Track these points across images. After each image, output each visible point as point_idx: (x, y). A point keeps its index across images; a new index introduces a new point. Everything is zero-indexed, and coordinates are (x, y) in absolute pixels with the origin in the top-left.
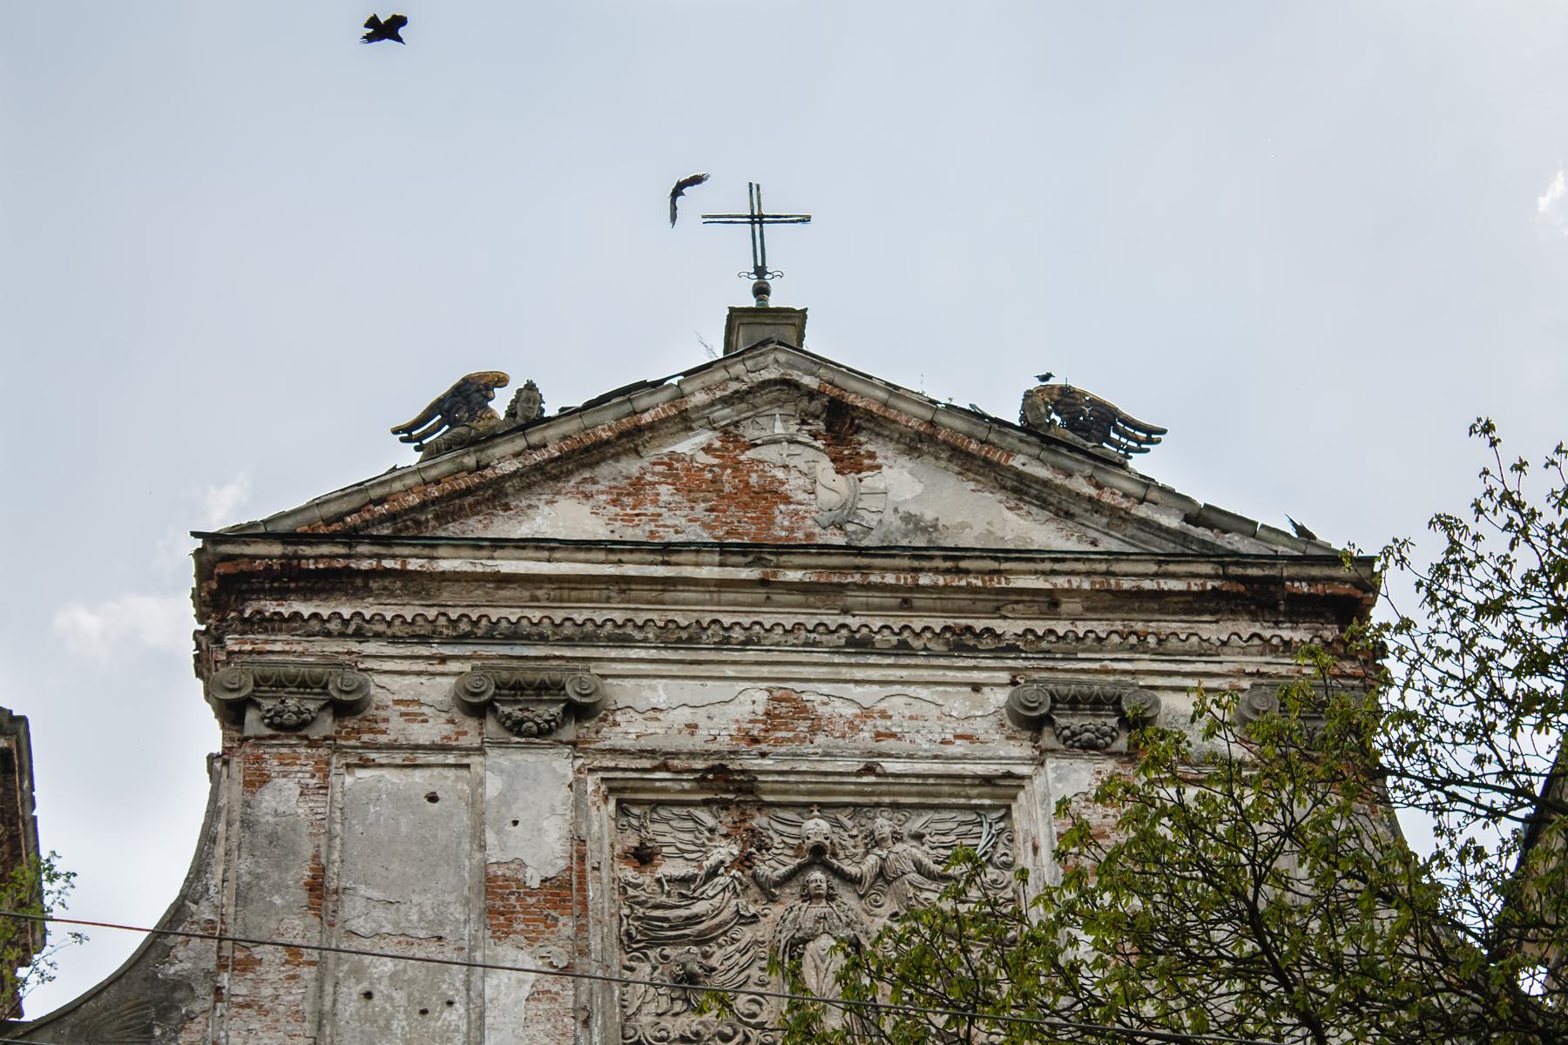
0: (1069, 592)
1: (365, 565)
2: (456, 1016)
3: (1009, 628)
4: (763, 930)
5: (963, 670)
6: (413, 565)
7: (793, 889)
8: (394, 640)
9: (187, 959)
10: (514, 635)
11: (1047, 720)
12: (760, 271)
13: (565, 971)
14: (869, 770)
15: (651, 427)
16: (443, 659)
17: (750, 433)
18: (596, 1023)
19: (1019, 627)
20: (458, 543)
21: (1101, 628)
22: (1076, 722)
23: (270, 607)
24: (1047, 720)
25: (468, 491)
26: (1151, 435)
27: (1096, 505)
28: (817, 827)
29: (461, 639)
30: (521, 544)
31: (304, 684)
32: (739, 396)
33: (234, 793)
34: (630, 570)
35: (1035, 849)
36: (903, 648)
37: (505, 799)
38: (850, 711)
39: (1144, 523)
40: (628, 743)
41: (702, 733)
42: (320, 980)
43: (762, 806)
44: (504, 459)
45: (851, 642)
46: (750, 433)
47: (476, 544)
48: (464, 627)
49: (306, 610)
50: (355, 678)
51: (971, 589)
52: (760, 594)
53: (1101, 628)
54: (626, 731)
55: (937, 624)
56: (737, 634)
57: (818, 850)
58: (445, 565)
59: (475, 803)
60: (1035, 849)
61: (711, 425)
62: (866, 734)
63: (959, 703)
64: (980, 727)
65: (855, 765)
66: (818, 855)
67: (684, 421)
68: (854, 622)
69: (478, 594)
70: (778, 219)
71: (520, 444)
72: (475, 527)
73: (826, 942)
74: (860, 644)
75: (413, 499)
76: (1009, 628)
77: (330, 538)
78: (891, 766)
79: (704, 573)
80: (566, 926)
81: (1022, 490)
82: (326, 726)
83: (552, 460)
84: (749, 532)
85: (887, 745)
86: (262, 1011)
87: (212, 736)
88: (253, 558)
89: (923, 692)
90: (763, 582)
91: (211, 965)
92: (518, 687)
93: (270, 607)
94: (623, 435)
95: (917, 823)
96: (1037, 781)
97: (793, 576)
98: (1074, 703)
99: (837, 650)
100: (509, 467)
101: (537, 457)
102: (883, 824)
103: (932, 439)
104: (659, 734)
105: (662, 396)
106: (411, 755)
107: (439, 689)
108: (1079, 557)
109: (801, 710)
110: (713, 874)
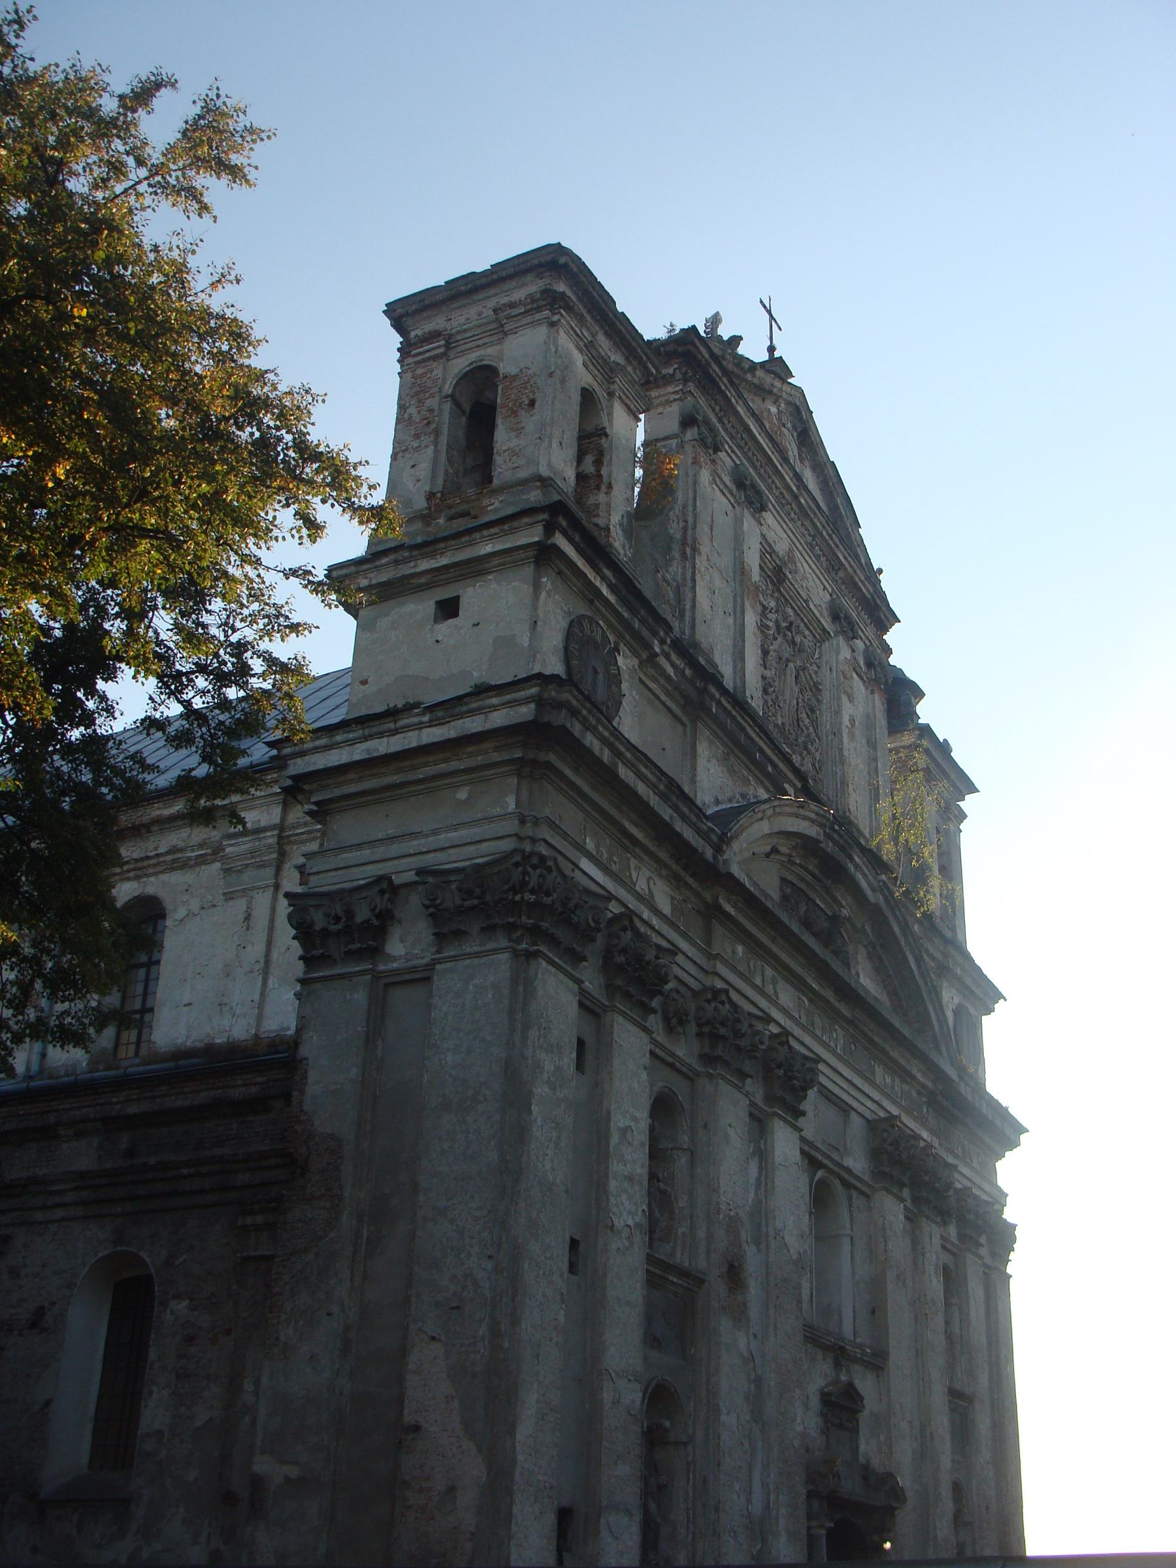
1: (723, 388)
6: (733, 401)
16: (733, 451)
35: (831, 670)
36: (818, 557)
45: (810, 544)
48: (743, 444)
58: (739, 409)
60: (831, 670)
63: (821, 591)
78: (812, 607)
83: (755, 385)
88: (700, 352)
91: (678, 536)
96: (835, 642)
97: (803, 501)
110: (770, 612)
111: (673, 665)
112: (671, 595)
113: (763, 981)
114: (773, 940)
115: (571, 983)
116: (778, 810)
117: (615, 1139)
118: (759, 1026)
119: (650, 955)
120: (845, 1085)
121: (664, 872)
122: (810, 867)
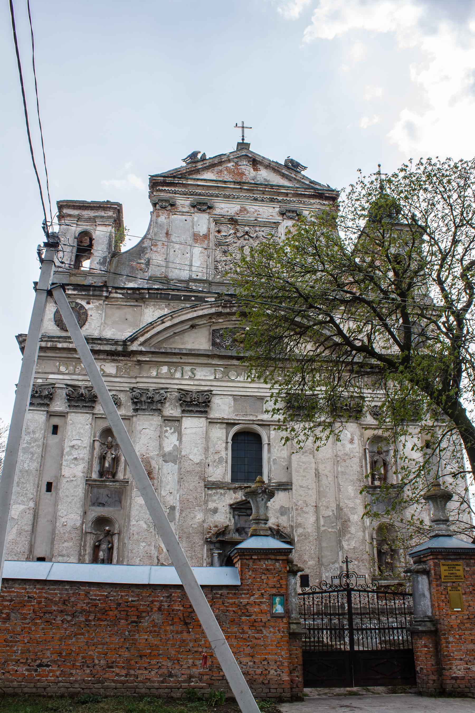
0: (290, 193)
2: (188, 255)
3: (280, 198)
4: (237, 245)
5: (272, 205)
6: (184, 182)
7: (242, 238)
8: (181, 194)
9: (147, 243)
10: (200, 195)
11: (285, 214)
12: (243, 136)
13: (206, 249)
14: (256, 220)
15: (224, 161)
17: (240, 163)
18: (210, 257)
19: (282, 198)
20: (191, 179)
21: (295, 199)
22: (289, 214)
23: (161, 188)
24: (285, 214)
25: (193, 171)
26: (305, 168)
27: (295, 179)
28: (247, 229)
29: (191, 195)
30: (202, 180)
31: (166, 201)
32: (238, 157)
33: (154, 218)
34: (219, 185)
37: (197, 221)
38: (253, 210)
39: (303, 183)
40: (217, 213)
41: (229, 212)
42: (167, 248)
43: (238, 225)
44: (199, 166)
46: (240, 163)
47: (194, 179)
49: (167, 189)
50: (174, 200)
51: (274, 192)
52: (240, 190)
53: (295, 199)
54: (217, 211)
55: (268, 197)
56: (236, 197)
57: (247, 232)
58: (189, 183)
59: (193, 221)
61: (234, 162)
62: (256, 214)
63: (271, 210)
64: (274, 214)
65: (254, 219)
66: (247, 233)
67: (229, 161)
68: (255, 196)
69: (194, 188)
70: (247, 128)
71: (202, 163)
72: (194, 176)
73: (247, 247)
74: (256, 199)
75: (185, 171)
76: (280, 198)
77: (171, 177)
78: (259, 219)
79: (231, 186)
80: (206, 242)
81: (283, 176)
82: (169, 208)
84: (239, 180)
85: (259, 216)
86: (158, 253)
87: (151, 208)
89: (265, 208)
90: (241, 188)
91: (150, 245)
92: (200, 203)
93: (161, 188)
94: (219, 162)
95: (263, 229)
98: (289, 211)
99: (252, 200)
100: (200, 167)
101: (205, 165)
102: (257, 229)
103: (269, 166)
104: (223, 212)
105: (226, 156)
106: (183, 213)
107: (188, 203)
108: (292, 187)
109: (245, 210)
110: (230, 235)
111: (120, 293)
112: (143, 266)
113: (182, 374)
114: (181, 358)
115: (42, 412)
116: (174, 316)
117: (67, 449)
118: (162, 391)
119: (82, 391)
120: (256, 390)
121: (108, 361)
122: (233, 319)
